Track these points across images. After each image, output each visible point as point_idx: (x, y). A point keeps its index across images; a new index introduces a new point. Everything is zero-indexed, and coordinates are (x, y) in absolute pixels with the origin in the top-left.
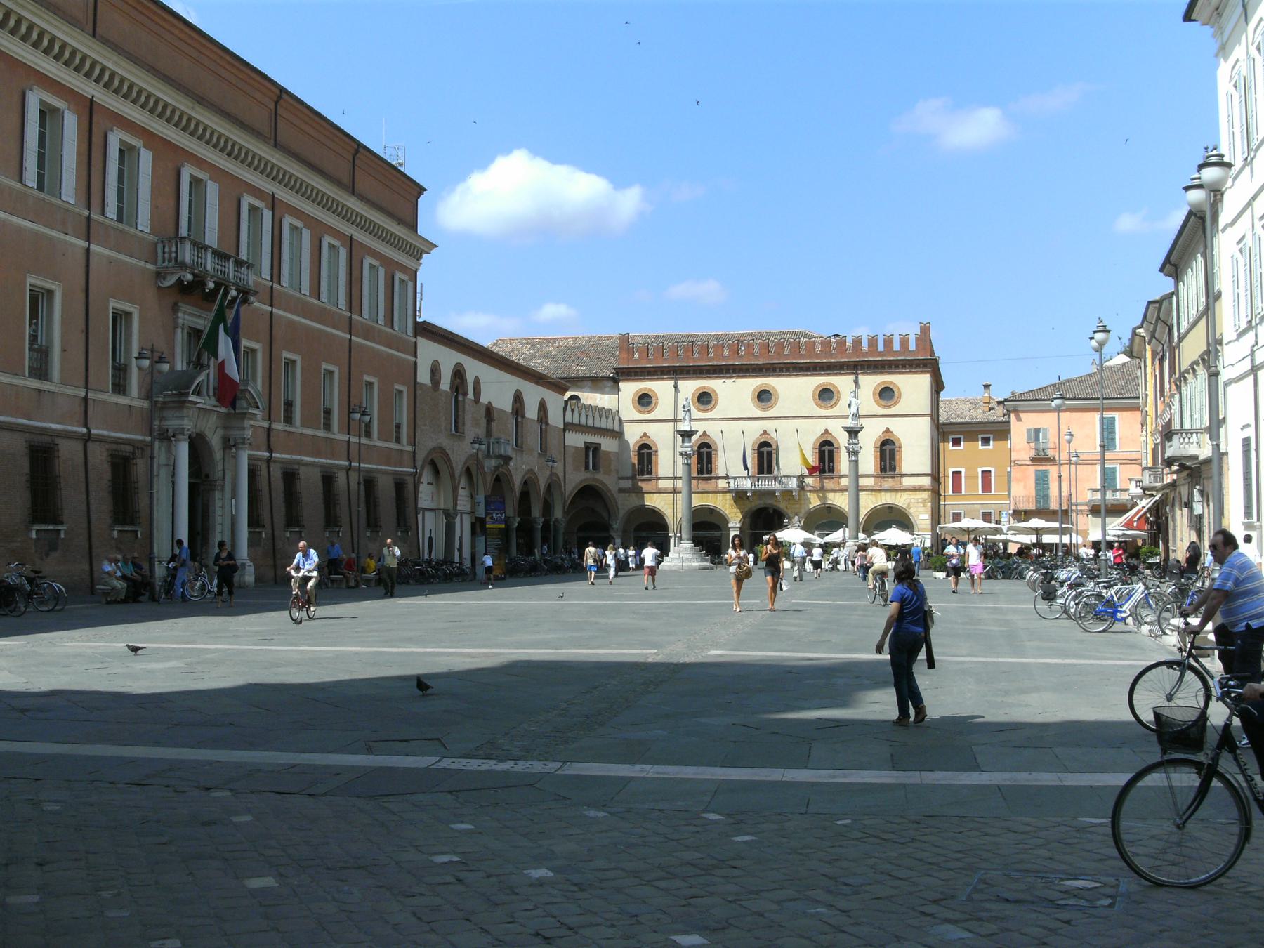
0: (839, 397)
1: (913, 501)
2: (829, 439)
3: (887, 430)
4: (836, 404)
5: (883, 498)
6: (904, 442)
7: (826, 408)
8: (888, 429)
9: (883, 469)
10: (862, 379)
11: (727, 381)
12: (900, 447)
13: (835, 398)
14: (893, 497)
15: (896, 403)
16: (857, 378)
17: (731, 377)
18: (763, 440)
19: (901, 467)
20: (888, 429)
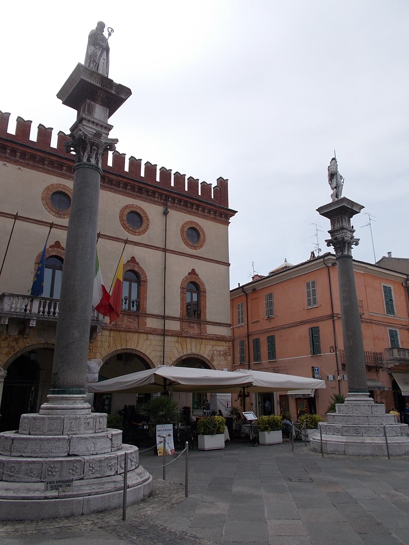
0: (148, 225)
1: (215, 352)
2: (136, 269)
3: (193, 272)
4: (145, 231)
5: (189, 347)
6: (208, 288)
7: (134, 233)
8: (193, 270)
9: (188, 314)
10: (172, 213)
11: (8, 164)
12: (205, 292)
13: (144, 225)
14: (198, 347)
15: (201, 246)
16: (166, 209)
17: (16, 162)
18: (54, 254)
19: (205, 316)
20: (193, 270)
